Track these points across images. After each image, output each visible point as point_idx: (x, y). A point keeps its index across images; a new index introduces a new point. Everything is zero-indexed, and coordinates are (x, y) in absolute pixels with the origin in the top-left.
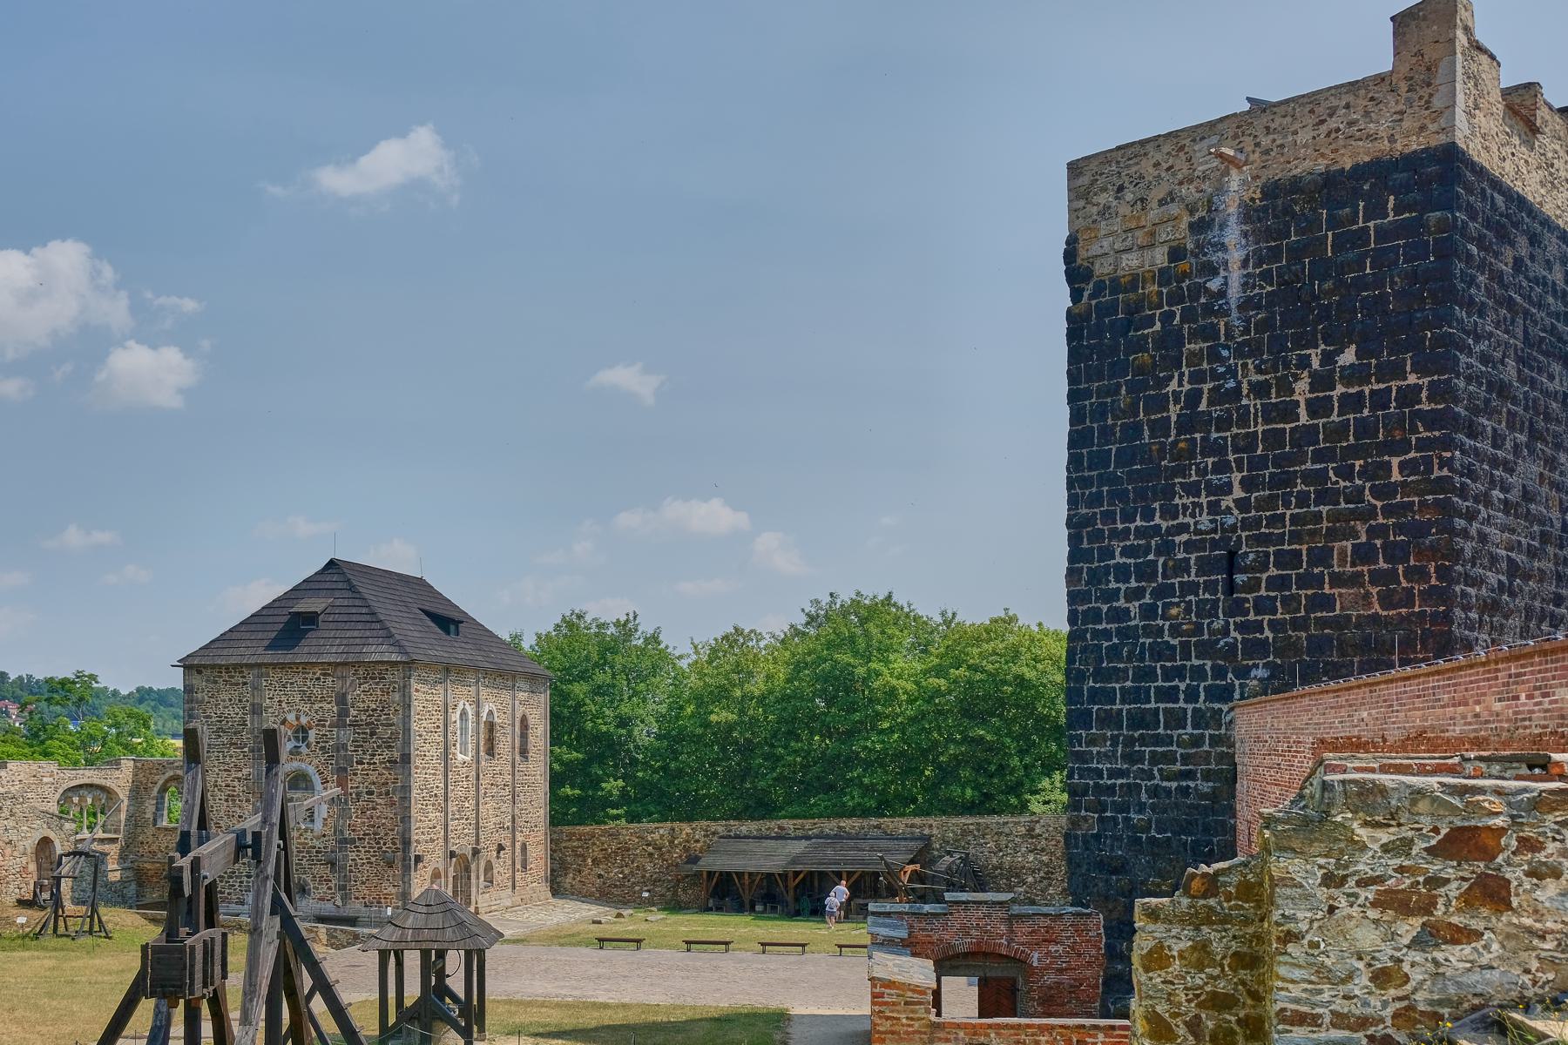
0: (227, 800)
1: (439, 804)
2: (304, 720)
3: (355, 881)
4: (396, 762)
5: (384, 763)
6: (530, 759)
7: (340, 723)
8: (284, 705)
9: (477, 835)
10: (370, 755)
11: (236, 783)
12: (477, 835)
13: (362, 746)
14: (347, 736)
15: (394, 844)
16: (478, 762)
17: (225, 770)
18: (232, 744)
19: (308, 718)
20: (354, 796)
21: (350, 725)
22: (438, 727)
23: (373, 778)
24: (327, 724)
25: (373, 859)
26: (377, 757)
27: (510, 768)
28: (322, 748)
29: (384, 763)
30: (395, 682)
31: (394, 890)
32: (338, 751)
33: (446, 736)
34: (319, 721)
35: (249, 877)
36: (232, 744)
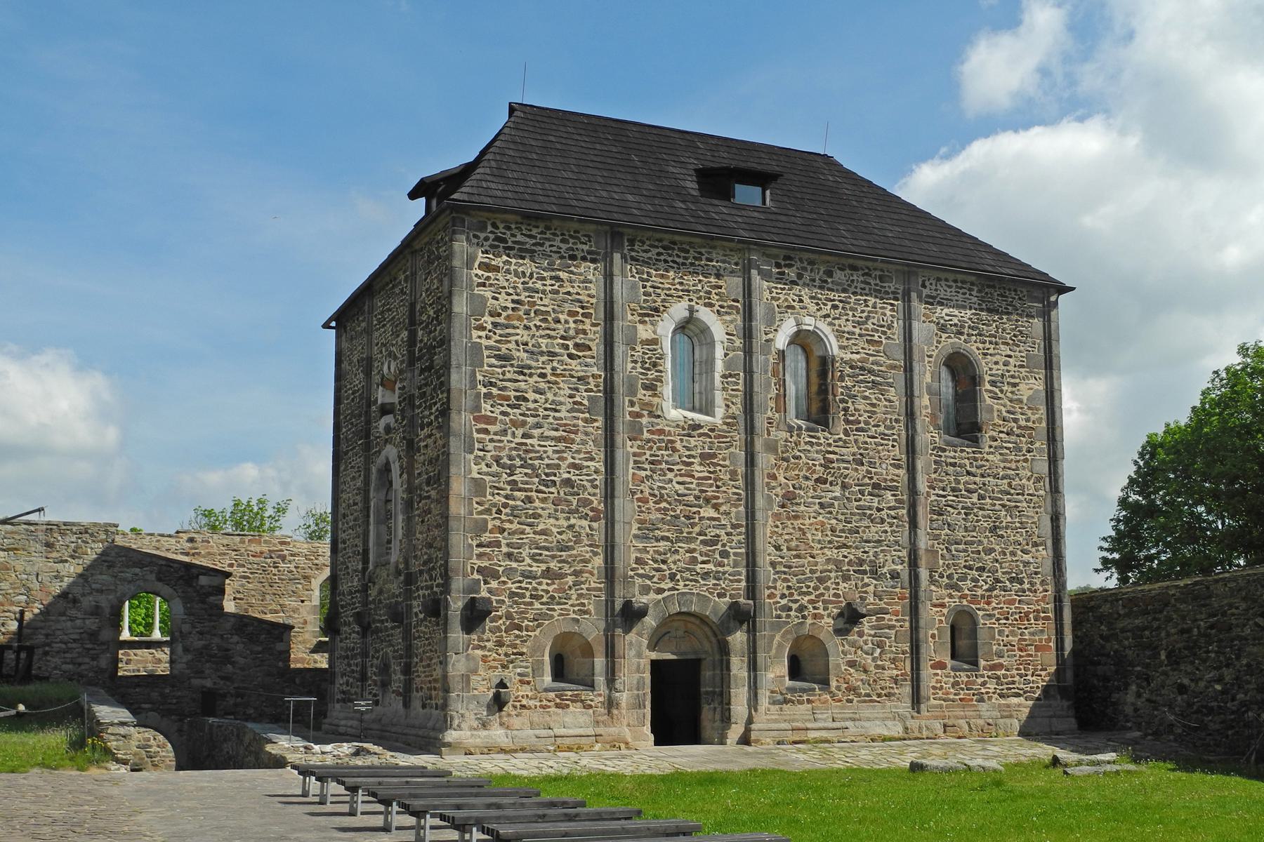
1: (586, 503)
6: (986, 442)
9: (752, 579)
12: (752, 579)
16: (750, 429)
26: (434, 409)
27: (898, 452)
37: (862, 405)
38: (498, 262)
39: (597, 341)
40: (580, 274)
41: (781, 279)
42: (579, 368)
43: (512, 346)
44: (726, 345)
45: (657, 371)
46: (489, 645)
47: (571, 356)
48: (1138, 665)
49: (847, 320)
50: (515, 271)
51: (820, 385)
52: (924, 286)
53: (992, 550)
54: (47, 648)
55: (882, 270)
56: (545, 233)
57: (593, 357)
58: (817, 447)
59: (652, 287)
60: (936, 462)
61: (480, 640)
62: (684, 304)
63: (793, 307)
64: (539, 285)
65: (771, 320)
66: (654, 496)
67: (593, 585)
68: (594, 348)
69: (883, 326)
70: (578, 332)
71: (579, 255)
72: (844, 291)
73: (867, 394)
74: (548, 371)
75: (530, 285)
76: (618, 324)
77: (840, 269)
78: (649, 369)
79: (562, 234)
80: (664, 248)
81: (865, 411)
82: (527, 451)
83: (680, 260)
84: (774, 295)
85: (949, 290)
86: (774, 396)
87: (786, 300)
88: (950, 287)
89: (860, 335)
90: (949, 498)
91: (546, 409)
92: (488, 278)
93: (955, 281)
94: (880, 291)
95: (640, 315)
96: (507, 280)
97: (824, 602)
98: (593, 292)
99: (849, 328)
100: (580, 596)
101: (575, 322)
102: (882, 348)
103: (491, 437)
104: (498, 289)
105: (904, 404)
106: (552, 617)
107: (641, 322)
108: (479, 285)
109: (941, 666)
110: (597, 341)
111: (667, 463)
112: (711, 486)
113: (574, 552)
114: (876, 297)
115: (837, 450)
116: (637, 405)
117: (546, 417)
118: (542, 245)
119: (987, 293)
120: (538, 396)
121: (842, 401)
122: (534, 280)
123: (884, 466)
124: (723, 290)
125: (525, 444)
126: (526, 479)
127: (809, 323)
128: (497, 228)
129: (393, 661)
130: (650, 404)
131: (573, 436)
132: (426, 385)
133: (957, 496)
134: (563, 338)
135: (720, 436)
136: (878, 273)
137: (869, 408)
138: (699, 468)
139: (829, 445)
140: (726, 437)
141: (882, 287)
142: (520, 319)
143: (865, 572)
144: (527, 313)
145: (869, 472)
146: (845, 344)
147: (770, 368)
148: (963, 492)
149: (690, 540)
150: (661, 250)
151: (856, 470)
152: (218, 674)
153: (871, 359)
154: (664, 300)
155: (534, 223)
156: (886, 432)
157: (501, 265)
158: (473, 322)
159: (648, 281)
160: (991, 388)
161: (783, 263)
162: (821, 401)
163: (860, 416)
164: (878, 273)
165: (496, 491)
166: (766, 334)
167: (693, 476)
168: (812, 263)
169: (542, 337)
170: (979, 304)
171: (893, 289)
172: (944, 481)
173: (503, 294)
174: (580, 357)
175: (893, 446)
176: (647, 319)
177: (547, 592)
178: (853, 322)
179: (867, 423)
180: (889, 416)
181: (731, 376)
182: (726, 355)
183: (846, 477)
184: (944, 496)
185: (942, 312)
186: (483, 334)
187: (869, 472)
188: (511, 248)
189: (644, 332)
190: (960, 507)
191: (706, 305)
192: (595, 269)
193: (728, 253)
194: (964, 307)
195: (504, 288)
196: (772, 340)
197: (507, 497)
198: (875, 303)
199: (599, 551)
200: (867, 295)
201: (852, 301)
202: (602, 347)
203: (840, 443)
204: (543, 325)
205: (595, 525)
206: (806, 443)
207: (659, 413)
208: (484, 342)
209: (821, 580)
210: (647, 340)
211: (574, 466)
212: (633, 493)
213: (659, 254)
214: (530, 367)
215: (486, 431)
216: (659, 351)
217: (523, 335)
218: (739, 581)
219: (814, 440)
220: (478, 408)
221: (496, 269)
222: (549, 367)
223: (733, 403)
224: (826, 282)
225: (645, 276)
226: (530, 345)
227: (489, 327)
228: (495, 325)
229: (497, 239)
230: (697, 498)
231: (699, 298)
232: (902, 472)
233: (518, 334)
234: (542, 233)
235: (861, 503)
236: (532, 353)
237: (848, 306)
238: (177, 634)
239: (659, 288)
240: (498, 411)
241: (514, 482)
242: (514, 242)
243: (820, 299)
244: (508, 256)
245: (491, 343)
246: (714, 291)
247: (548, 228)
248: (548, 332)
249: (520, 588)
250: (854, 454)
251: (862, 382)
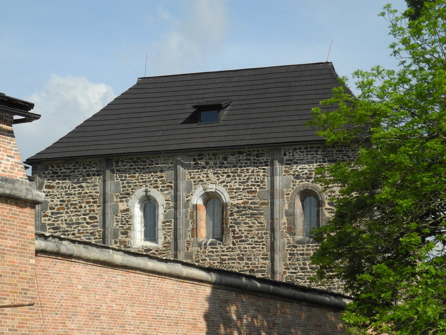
37: (244, 227)
38: (54, 183)
39: (100, 214)
40: (92, 183)
41: (196, 167)
42: (91, 228)
44: (165, 207)
45: (128, 225)
47: (88, 223)
49: (235, 182)
50: (62, 186)
52: (285, 155)
55: (258, 151)
56: (76, 166)
57: (98, 222)
58: (215, 254)
59: (127, 183)
60: (290, 254)
62: (143, 189)
63: (202, 181)
64: (72, 192)
65: (189, 190)
68: (98, 218)
69: (258, 182)
70: (90, 211)
71: (92, 173)
72: (234, 166)
73: (247, 221)
74: (76, 231)
75: (69, 192)
76: (108, 204)
77: (232, 155)
78: (125, 224)
79: (84, 165)
80: (133, 162)
81: (245, 231)
83: (141, 167)
84: (192, 176)
85: (301, 154)
86: (190, 229)
87: (199, 177)
88: (302, 152)
89: (243, 189)
90: (299, 274)
92: (49, 192)
93: (306, 148)
94: (256, 163)
95: (120, 198)
96: (58, 191)
98: (98, 190)
101: (89, 206)
102: (257, 194)
104: (53, 197)
105: (269, 224)
107: (121, 201)
110: (100, 214)
114: (254, 166)
115: (228, 253)
116: (118, 243)
118: (73, 172)
119: (328, 151)
121: (231, 227)
122: (70, 189)
123: (257, 259)
124: (164, 178)
127: (211, 188)
128: (54, 167)
130: (124, 242)
133: (304, 272)
134: (84, 215)
136: (255, 153)
137: (248, 229)
139: (223, 251)
140: (164, 253)
141: (258, 160)
142: (63, 209)
144: (67, 205)
145: (247, 264)
146: (234, 195)
147: (189, 215)
148: (309, 270)
150: (132, 164)
151: (239, 263)
153: (250, 201)
154: (133, 189)
155: (70, 162)
156: (259, 240)
157: (55, 185)
158: (42, 213)
159: (125, 180)
160: (330, 207)
161: (197, 158)
163: (242, 233)
164: (255, 153)
166: (187, 197)
168: (215, 155)
169: (74, 216)
170: (323, 159)
171: (265, 160)
172: (296, 264)
173: (56, 199)
174: (91, 223)
175: (262, 248)
176: (124, 199)
178: (239, 182)
179: (246, 237)
180: (260, 232)
181: (168, 222)
182: (165, 211)
183: (233, 267)
185: (297, 168)
186: (46, 218)
187: (247, 264)
188: (60, 176)
189: (122, 206)
190: (306, 277)
191: (155, 187)
192: (99, 179)
193: (167, 158)
194: (312, 163)
195: (56, 195)
196: (190, 200)
198: (253, 170)
200: (248, 166)
201: (239, 171)
202: (102, 217)
203: (230, 250)
204: (74, 210)
206: (209, 252)
207: (128, 246)
208: (47, 222)
210: (124, 210)
213: (131, 166)
214: (67, 231)
216: (130, 214)
217: (65, 216)
219: (214, 250)
221: (53, 187)
222: (76, 230)
223: (168, 236)
224: (223, 163)
225: (123, 178)
226: (68, 220)
227: (50, 214)
228: (52, 213)
229: (54, 173)
231: (151, 184)
232: (268, 262)
233: (63, 216)
234: (74, 166)
236: (69, 224)
237: (236, 175)
239: (130, 183)
242: (61, 173)
243: (220, 174)
244: (59, 180)
245: (51, 222)
246: (159, 180)
247: (77, 163)
248: (77, 213)
250: (238, 255)
251: (244, 215)
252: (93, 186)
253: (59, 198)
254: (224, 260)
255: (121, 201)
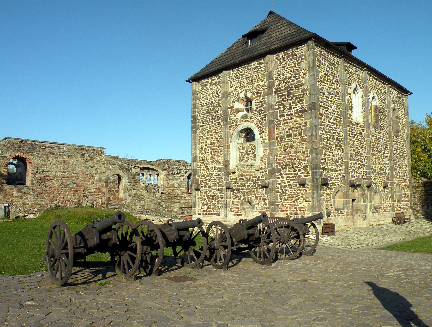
0: (211, 153)
1: (341, 146)
2: (249, 95)
3: (281, 199)
4: (305, 111)
5: (297, 113)
7: (270, 92)
8: (238, 89)
10: (289, 109)
11: (216, 142)
12: (369, 173)
13: (283, 104)
14: (273, 99)
15: (306, 170)
17: (211, 135)
18: (213, 119)
19: (251, 94)
20: (279, 139)
21: (275, 92)
22: (338, 93)
23: (290, 125)
24: (262, 94)
25: (292, 182)
26: (293, 110)
28: (260, 111)
29: (297, 113)
30: (302, 55)
31: (305, 204)
32: (269, 110)
33: (344, 101)
34: (257, 93)
35: (222, 198)
36: (213, 119)
42: (337, 100)
43: (325, 89)
46: (325, 195)
48: (428, 200)
51: (375, 114)
53: (401, 167)
54: (85, 195)
59: (349, 76)
61: (323, 193)
66: (352, 145)
67: (343, 175)
68: (340, 94)
82: (330, 127)
83: (353, 69)
91: (332, 113)
95: (348, 85)
97: (380, 181)
98: (339, 75)
99: (379, 98)
100: (341, 178)
103: (322, 121)
106: (336, 185)
108: (318, 66)
109: (395, 201)
111: (354, 134)
112: (362, 143)
113: (339, 163)
115: (379, 134)
117: (332, 116)
120: (331, 108)
125: (329, 124)
126: (330, 137)
129: (255, 201)
131: (338, 123)
132: (284, 101)
135: (362, 128)
138: (359, 137)
142: (326, 80)
143: (384, 172)
149: (358, 160)
152: (140, 204)
159: (348, 74)
162: (375, 119)
165: (324, 140)
167: (358, 140)
177: (335, 176)
184: (394, 151)
186: (319, 84)
188: (323, 55)
195: (322, 69)
197: (327, 143)
199: (344, 163)
203: (380, 133)
205: (343, 154)
209: (379, 174)
211: (339, 134)
212: (349, 144)
213: (350, 66)
215: (321, 118)
218: (366, 174)
220: (320, 110)
227: (320, 82)
230: (359, 147)
235: (383, 151)
238: (126, 190)
240: (323, 112)
241: (327, 138)
242: (324, 53)
245: (320, 87)
249: (330, 175)
252: (337, 71)
253: (323, 71)
254: (379, 138)
255: (349, 87)
